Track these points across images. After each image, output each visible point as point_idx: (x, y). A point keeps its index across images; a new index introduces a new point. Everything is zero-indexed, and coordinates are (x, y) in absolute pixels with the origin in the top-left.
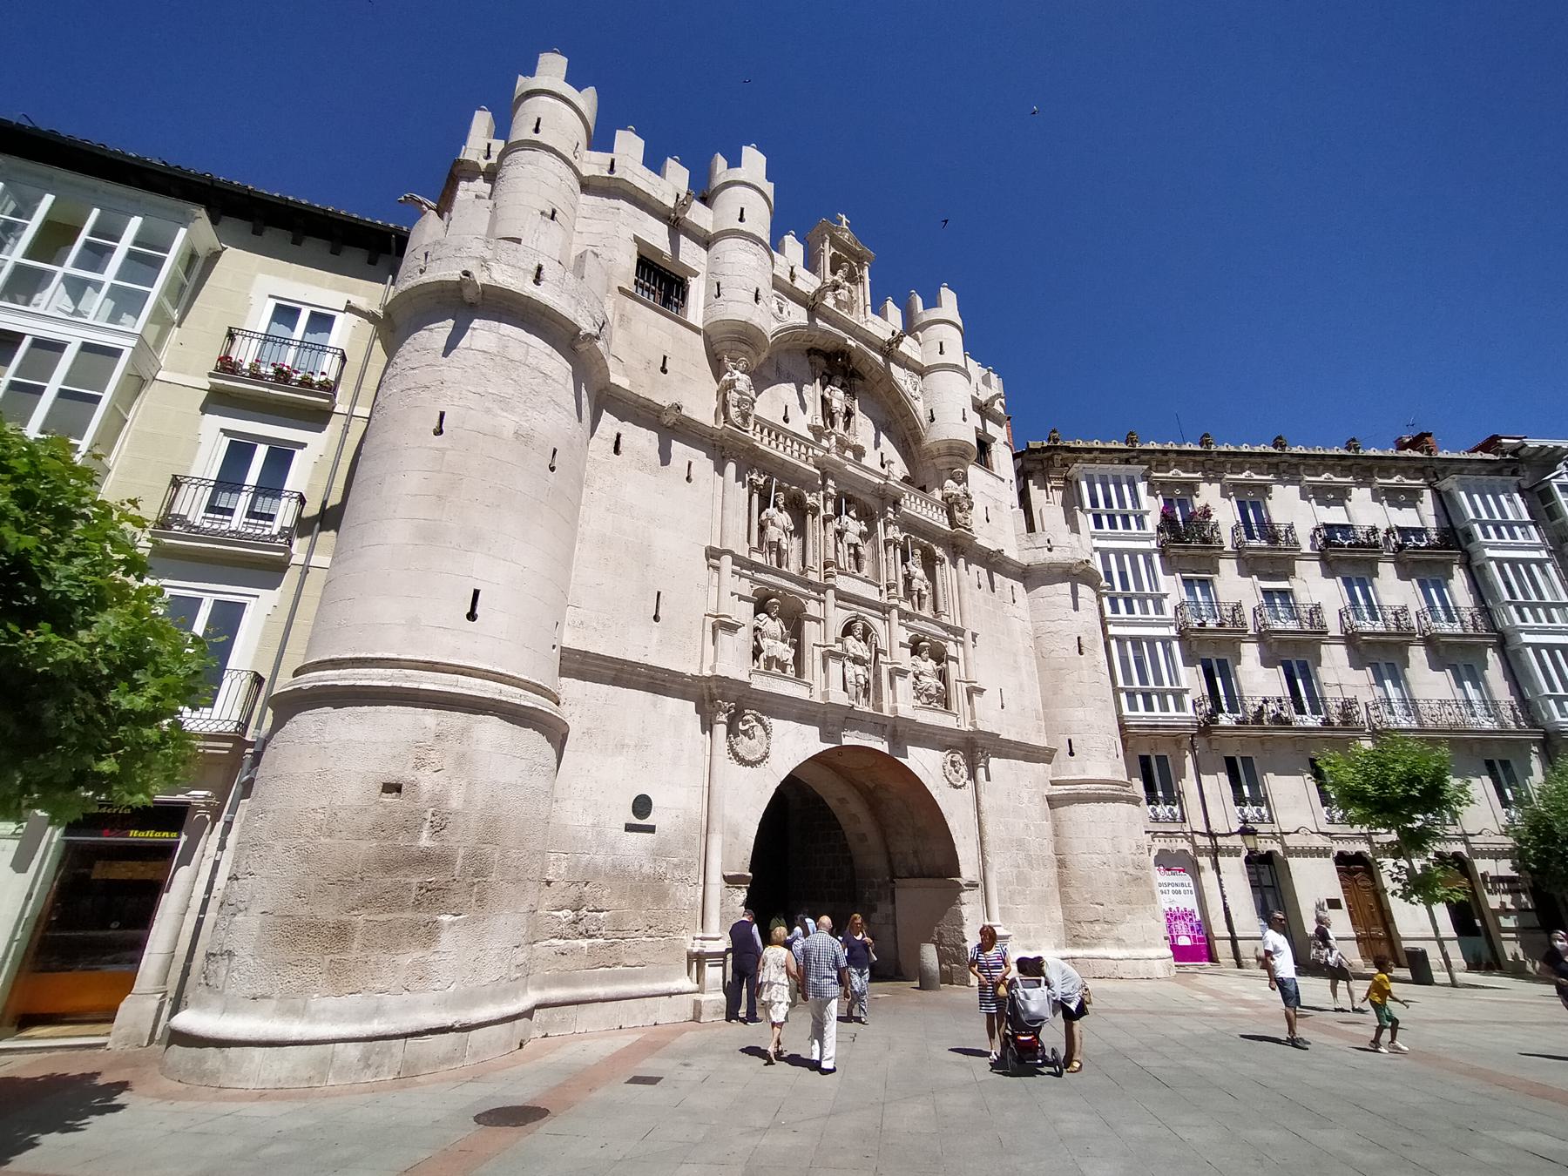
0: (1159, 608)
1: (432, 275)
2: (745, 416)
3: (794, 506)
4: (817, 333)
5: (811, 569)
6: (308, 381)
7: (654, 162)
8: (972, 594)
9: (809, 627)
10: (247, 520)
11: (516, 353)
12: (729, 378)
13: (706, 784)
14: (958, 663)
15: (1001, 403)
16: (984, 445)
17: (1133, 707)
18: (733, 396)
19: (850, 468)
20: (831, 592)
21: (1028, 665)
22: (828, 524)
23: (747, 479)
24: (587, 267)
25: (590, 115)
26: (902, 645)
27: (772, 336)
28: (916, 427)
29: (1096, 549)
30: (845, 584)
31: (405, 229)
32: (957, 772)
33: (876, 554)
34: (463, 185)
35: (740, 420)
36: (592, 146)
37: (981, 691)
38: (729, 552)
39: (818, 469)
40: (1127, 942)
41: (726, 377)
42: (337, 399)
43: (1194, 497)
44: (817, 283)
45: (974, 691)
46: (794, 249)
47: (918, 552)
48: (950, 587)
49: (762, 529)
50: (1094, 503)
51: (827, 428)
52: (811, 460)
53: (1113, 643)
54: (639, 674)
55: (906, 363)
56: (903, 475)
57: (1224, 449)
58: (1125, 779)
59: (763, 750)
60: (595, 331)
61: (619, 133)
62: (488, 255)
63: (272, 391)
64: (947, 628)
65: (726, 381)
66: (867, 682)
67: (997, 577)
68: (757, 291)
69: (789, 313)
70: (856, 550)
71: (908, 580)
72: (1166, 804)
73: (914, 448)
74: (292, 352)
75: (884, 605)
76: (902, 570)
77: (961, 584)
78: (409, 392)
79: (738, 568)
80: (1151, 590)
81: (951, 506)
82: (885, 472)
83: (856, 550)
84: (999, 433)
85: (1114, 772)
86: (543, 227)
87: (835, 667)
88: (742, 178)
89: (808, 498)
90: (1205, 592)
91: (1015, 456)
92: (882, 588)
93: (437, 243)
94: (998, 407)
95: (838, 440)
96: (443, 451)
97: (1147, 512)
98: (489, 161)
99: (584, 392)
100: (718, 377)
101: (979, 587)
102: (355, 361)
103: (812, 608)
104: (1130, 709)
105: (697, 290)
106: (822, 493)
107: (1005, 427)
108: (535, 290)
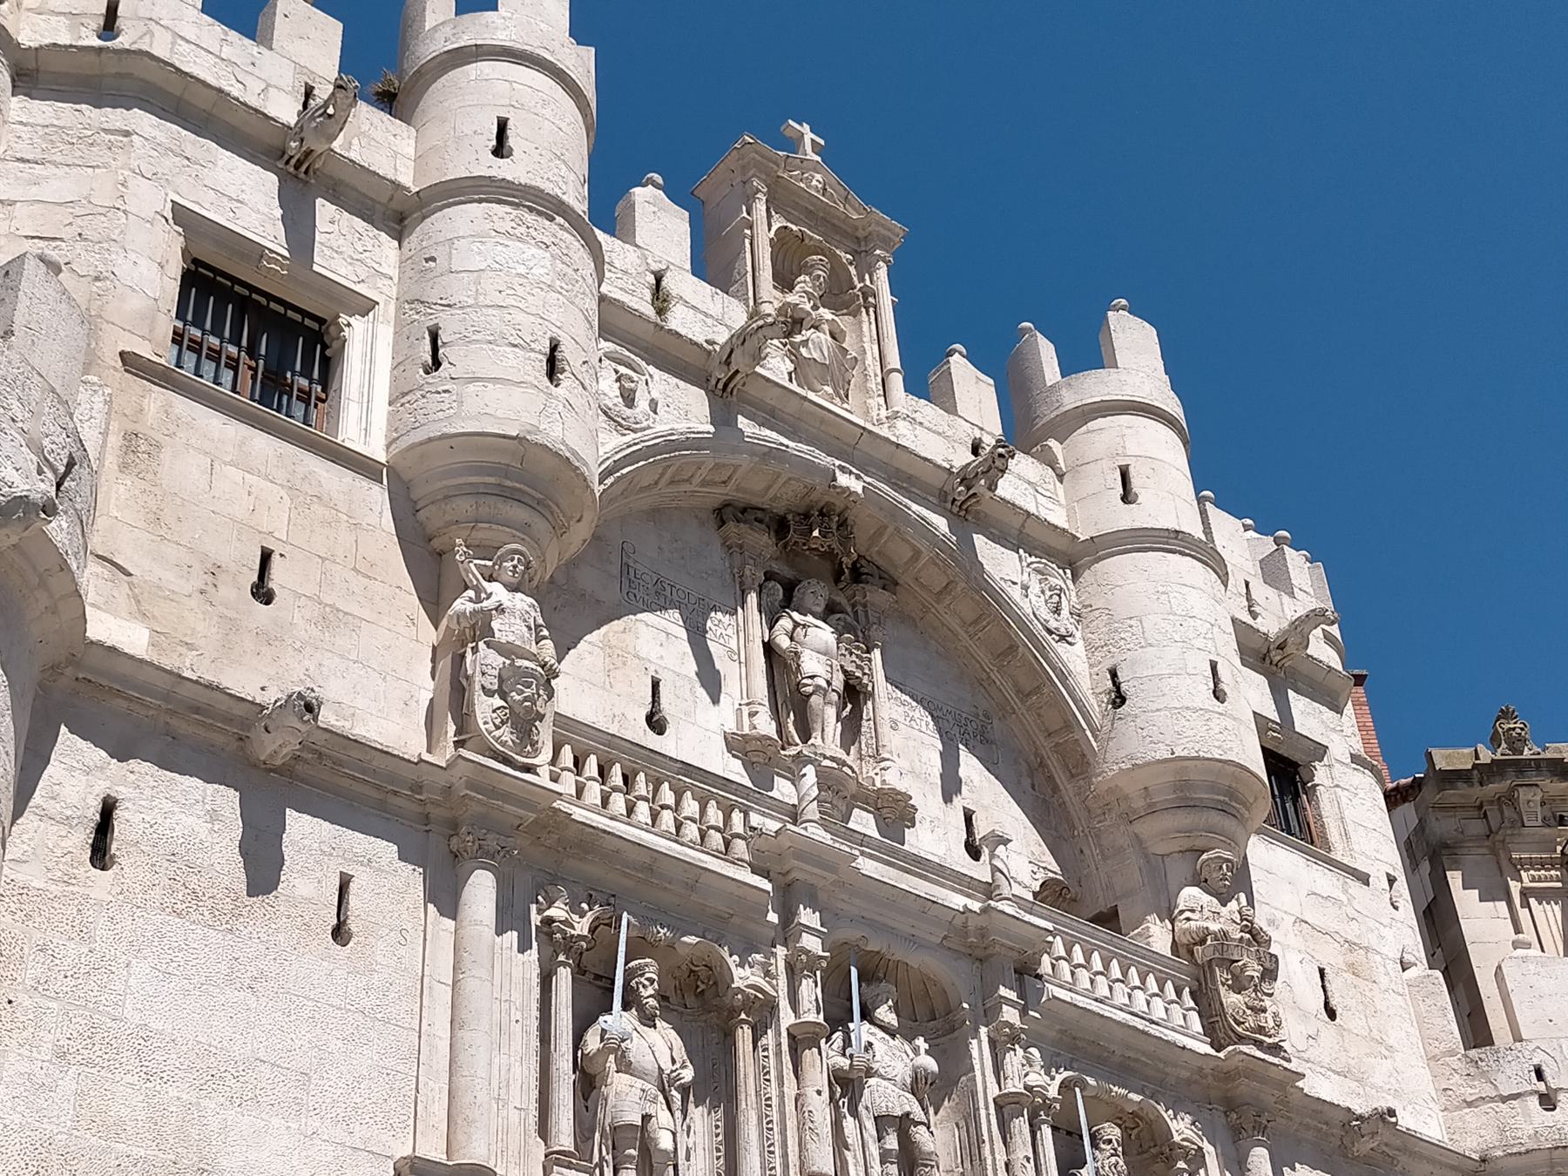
2: (524, 723)
3: (691, 1000)
4: (744, 460)
12: (470, 607)
15: (1328, 638)
18: (484, 662)
19: (868, 867)
22: (809, 1055)
23: (535, 919)
28: (1069, 724)
35: (506, 734)
39: (765, 874)
41: (462, 604)
44: (738, 316)
47: (1112, 1132)
49: (588, 1083)
52: (740, 847)
60: (43, 488)
65: (460, 616)
68: (554, 348)
69: (654, 405)
70: (906, 1141)
73: (1068, 789)
82: (980, 871)
88: (502, 38)
89: (738, 973)
91: (1394, 798)
94: (1322, 651)
100: (434, 601)
106: (781, 951)
107: (1349, 709)
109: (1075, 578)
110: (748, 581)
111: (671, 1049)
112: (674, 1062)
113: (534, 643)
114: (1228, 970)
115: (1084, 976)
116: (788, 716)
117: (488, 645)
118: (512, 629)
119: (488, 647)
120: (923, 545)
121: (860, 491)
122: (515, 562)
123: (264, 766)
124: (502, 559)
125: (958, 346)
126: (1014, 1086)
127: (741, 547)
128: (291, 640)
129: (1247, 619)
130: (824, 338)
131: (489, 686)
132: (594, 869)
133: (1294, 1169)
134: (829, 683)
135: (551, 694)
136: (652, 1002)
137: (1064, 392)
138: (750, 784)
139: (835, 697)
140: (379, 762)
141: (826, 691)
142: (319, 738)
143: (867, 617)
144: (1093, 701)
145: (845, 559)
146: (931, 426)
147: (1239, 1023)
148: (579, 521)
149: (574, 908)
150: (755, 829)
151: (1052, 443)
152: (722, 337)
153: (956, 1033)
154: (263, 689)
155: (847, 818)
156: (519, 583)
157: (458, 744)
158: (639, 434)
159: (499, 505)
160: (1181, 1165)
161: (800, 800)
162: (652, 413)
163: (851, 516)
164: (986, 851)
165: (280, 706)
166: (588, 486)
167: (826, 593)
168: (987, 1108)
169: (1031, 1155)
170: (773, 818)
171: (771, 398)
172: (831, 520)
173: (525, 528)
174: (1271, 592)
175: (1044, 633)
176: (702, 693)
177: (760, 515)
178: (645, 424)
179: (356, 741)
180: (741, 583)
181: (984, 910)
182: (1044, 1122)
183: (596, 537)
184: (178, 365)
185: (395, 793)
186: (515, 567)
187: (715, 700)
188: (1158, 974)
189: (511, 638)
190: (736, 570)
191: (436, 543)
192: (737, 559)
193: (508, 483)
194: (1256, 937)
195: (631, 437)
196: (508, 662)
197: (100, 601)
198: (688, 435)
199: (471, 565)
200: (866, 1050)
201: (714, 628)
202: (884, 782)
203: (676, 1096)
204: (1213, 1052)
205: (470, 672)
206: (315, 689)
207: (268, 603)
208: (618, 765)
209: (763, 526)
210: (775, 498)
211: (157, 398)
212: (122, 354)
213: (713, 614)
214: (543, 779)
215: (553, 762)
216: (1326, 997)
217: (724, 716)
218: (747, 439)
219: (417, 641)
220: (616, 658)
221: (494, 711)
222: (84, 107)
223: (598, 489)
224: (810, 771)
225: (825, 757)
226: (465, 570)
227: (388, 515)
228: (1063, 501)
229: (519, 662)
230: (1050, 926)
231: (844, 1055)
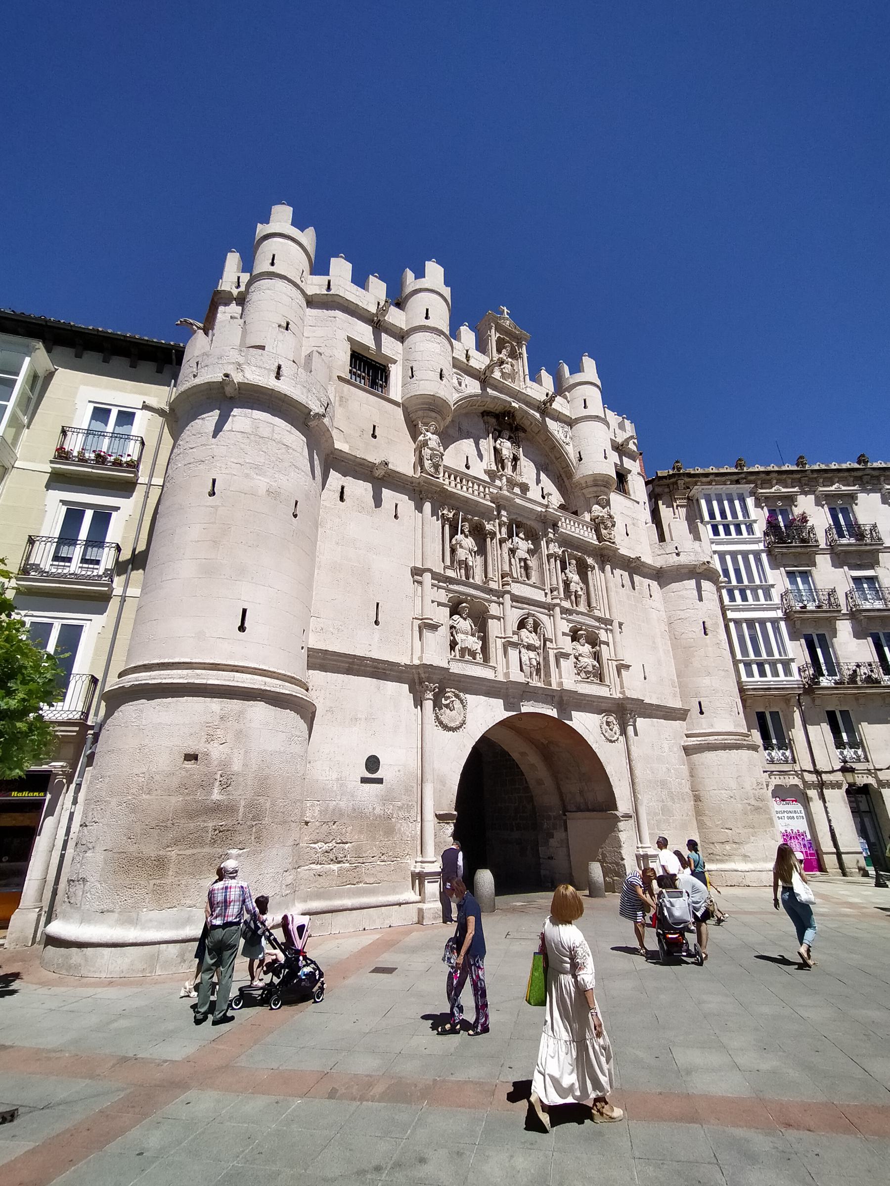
0: (768, 596)
1: (202, 378)
2: (436, 467)
6: (119, 461)
7: (359, 280)
9: (492, 625)
10: (81, 565)
11: (265, 431)
12: (423, 439)
13: (420, 746)
14: (608, 646)
15: (634, 443)
16: (622, 476)
17: (750, 674)
18: (426, 452)
19: (518, 501)
20: (508, 597)
21: (664, 645)
22: (504, 545)
23: (440, 514)
24: (314, 363)
25: (311, 248)
26: (564, 634)
27: (454, 405)
28: (568, 466)
29: (715, 552)
30: (518, 589)
31: (182, 345)
32: (611, 730)
34: (221, 309)
35: (432, 470)
36: (314, 272)
39: (494, 503)
40: (753, 857)
41: (421, 438)
42: (139, 474)
43: (793, 506)
45: (622, 667)
46: (468, 336)
47: (574, 562)
49: (453, 551)
50: (712, 516)
51: (499, 471)
53: (732, 625)
54: (366, 665)
55: (558, 417)
56: (560, 503)
57: (816, 467)
58: (745, 731)
59: (460, 719)
60: (321, 411)
61: (333, 260)
62: (241, 360)
63: (94, 471)
64: (598, 619)
65: (420, 441)
66: (539, 663)
67: (637, 578)
69: (466, 386)
70: (525, 563)
71: (567, 584)
72: (779, 749)
74: (106, 441)
75: (549, 604)
76: (562, 577)
77: (609, 585)
78: (191, 466)
79: (436, 582)
80: (761, 581)
81: (597, 525)
82: (545, 502)
83: (525, 563)
84: (633, 467)
85: (736, 726)
86: (281, 337)
87: (513, 653)
89: (487, 526)
90: (805, 581)
91: (647, 483)
92: (546, 591)
93: (205, 354)
94: (632, 446)
95: (507, 478)
96: (216, 508)
97: (755, 521)
98: (239, 290)
99: (316, 457)
101: (623, 586)
102: (151, 444)
103: (494, 609)
104: (748, 676)
105: (396, 373)
106: (497, 521)
107: (638, 461)
108: (277, 384)
109: (571, 428)
120: (533, 421)
124: (430, 426)
125: (543, 368)
126: (551, 552)
129: (614, 439)
130: (509, 366)
135: (442, 460)
136: (467, 533)
137: (570, 379)
140: (403, 476)
142: (388, 471)
149: (449, 511)
151: (567, 393)
152: (483, 367)
155: (513, 490)
157: (421, 472)
160: (589, 569)
164: (546, 497)
171: (495, 383)
176: (479, 459)
184: (351, 378)
187: (482, 461)
194: (611, 517)
195: (461, 394)
197: (337, 439)
203: (473, 554)
210: (496, 410)
211: (347, 387)
212: (338, 376)
214: (441, 481)
215: (443, 476)
217: (484, 465)
222: (324, 311)
223: (453, 408)
224: (504, 478)
227: (403, 416)
229: (435, 452)
230: (561, 515)
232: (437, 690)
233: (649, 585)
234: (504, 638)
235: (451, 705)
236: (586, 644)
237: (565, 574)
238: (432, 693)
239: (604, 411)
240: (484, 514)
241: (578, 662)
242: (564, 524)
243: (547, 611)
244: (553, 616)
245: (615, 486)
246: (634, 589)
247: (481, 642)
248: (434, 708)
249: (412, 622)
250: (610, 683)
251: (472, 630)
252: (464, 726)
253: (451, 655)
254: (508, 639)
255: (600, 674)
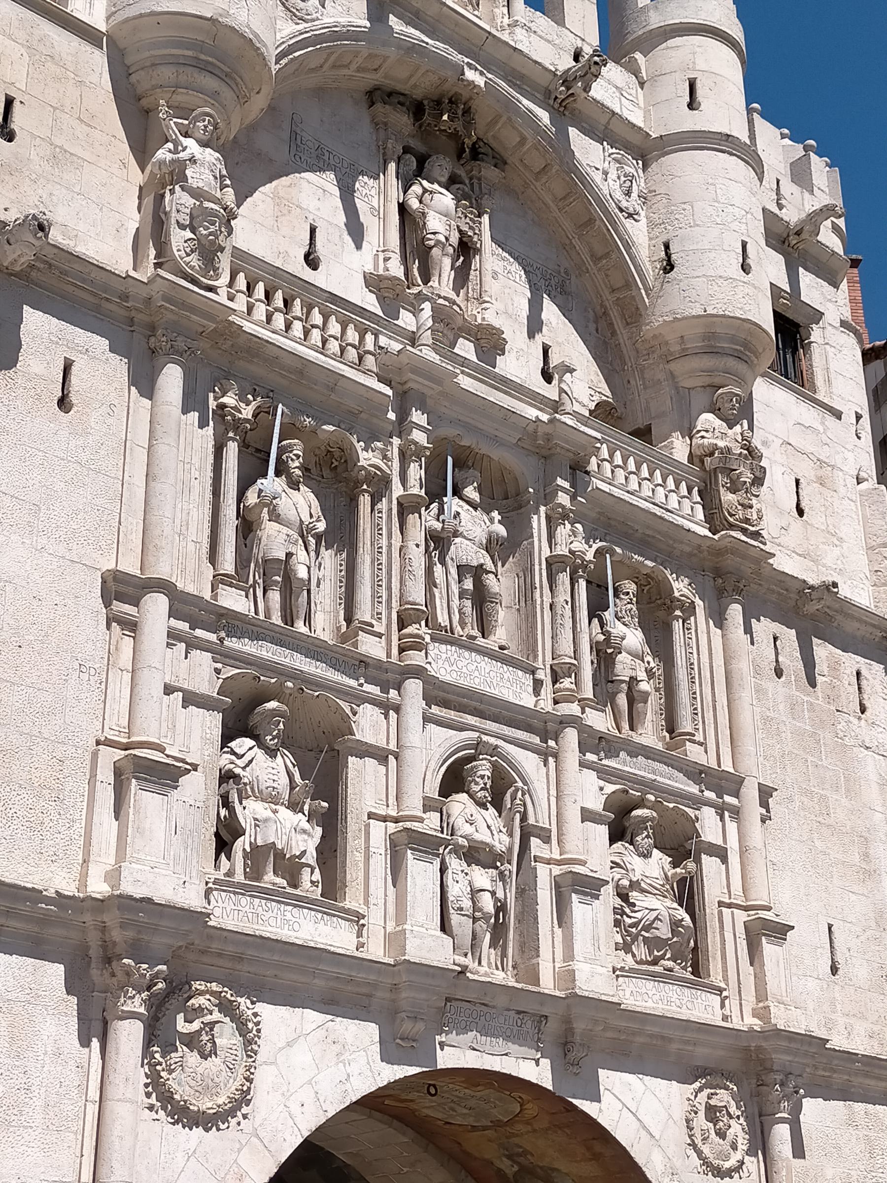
3: (326, 473)
4: (392, 52)
5: (367, 628)
8: (759, 690)
12: (169, 156)
14: (724, 859)
15: (835, 228)
19: (466, 382)
20: (414, 687)
22: (412, 519)
26: (587, 816)
27: (279, 58)
28: (629, 284)
32: (721, 1134)
33: (527, 592)
35: (194, 260)
37: (780, 931)
38: (164, 586)
39: (388, 383)
41: (163, 154)
47: (631, 587)
48: (706, 674)
51: (411, 284)
52: (370, 361)
56: (597, 398)
64: (697, 774)
65: (162, 163)
66: (501, 908)
67: (822, 651)
70: (479, 584)
73: (623, 334)
76: (589, 632)
79: (184, 626)
82: (550, 392)
89: (363, 455)
91: (868, 356)
92: (540, 675)
101: (779, 673)
106: (396, 441)
107: (844, 285)
109: (645, 168)
110: (389, 153)
111: (310, 507)
112: (311, 516)
113: (218, 190)
114: (728, 476)
115: (620, 474)
116: (414, 263)
117: (183, 188)
118: (202, 177)
119: (183, 190)
120: (528, 133)
121: (482, 85)
122: (206, 123)
123: (6, 271)
124: (196, 120)
126: (562, 550)
127: (386, 124)
128: (28, 173)
129: (775, 210)
131: (182, 221)
132: (257, 370)
133: (759, 620)
134: (447, 239)
135: (230, 231)
136: (298, 472)
137: (652, 13)
138: (381, 314)
139: (450, 250)
141: (444, 245)
142: (51, 252)
143: (480, 188)
144: (648, 265)
145: (466, 140)
146: (543, 35)
147: (731, 515)
148: (258, 93)
149: (242, 398)
150: (383, 348)
151: (638, 56)
153: (523, 510)
154: (6, 210)
155: (453, 345)
156: (209, 140)
157: (157, 265)
158: (309, 24)
159: (196, 75)
160: (678, 613)
161: (418, 328)
162: (320, 7)
163: (474, 104)
164: (556, 376)
165: (19, 224)
166: (266, 65)
167: (449, 167)
168: (540, 565)
169: (569, 600)
170: (397, 340)
172: (458, 107)
173: (215, 95)
174: (795, 189)
175: (617, 210)
176: (348, 239)
177: (402, 99)
178: (314, 16)
179: (77, 256)
180: (384, 154)
181: (552, 421)
182: (581, 577)
183: (272, 109)
185: (107, 299)
186: (206, 127)
187: (359, 247)
188: (676, 476)
189: (201, 185)
190: (381, 143)
191: (144, 102)
192: (382, 134)
193: (203, 57)
194: (752, 453)
195: (302, 26)
196: (198, 203)
198: (349, 28)
199: (171, 122)
200: (455, 517)
201: (360, 189)
202: (483, 319)
203: (312, 541)
204: (710, 535)
205: (168, 209)
206: (47, 213)
207: (10, 140)
208: (280, 291)
209: (404, 109)
210: (415, 85)
213: (360, 178)
215: (231, 285)
216: (798, 500)
218: (395, 35)
219: (127, 181)
220: (283, 206)
221: (185, 242)
223: (275, 68)
224: (427, 306)
225: (440, 297)
226: (166, 126)
227: (107, 76)
228: (642, 105)
229: (207, 204)
230: (599, 436)
231: (438, 520)
232: (161, 985)
233: (858, 674)
234: (396, 821)
235: (205, 1038)
236: (656, 852)
237: (602, 625)
238: (145, 995)
239: (751, 122)
240: (354, 415)
241: (627, 910)
242: (607, 466)
243: (536, 740)
244: (556, 756)
245: (770, 355)
246: (812, 683)
247: (319, 831)
248: (148, 1043)
249: (95, 755)
250: (726, 979)
251: (292, 788)
252: (245, 1110)
253: (217, 867)
254: (408, 825)
255: (695, 949)
